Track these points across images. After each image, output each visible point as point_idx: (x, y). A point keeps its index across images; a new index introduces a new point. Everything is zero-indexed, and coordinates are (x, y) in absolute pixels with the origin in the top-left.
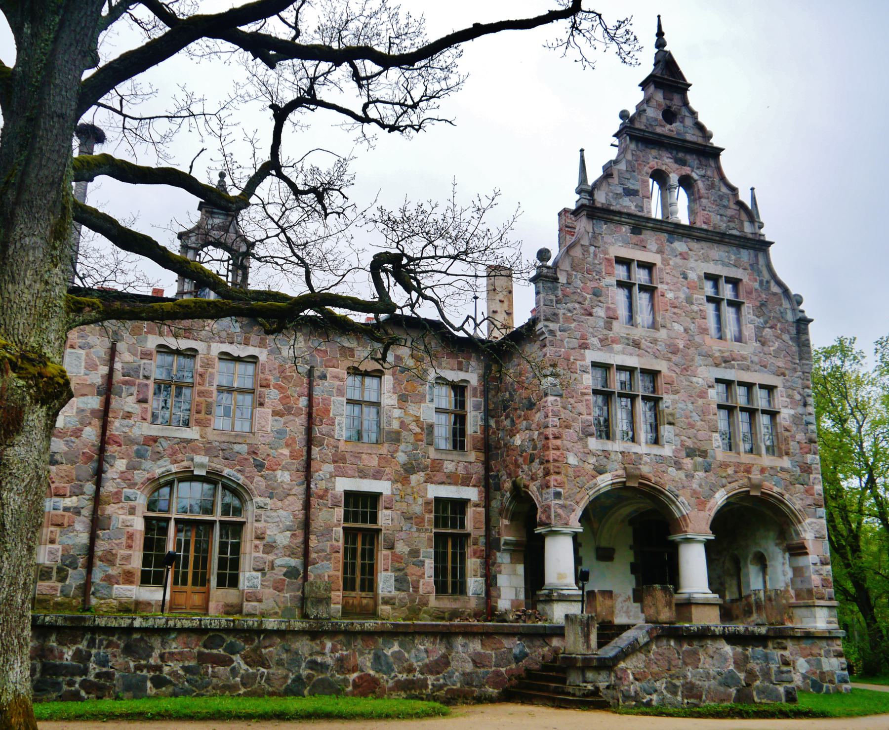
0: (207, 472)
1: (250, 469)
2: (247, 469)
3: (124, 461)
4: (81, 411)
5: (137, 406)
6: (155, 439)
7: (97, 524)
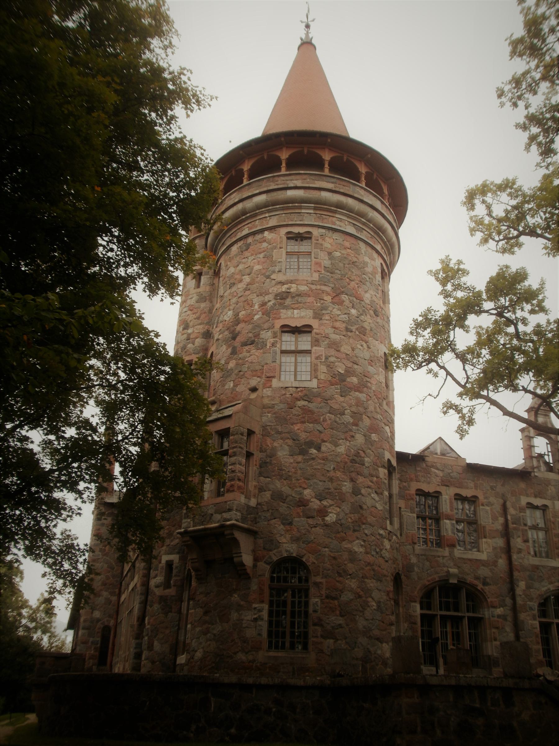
4: (494, 548)
7: (517, 626)
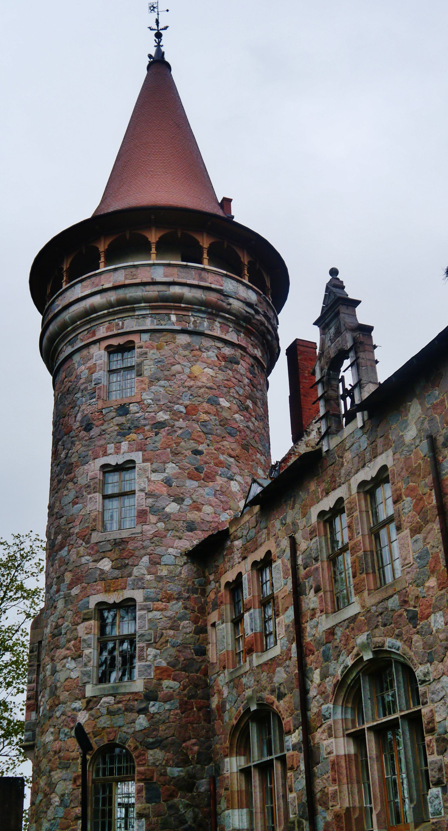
0: (374, 652)
1: (407, 628)
2: (404, 630)
3: (318, 671)
5: (315, 598)
6: (331, 632)
